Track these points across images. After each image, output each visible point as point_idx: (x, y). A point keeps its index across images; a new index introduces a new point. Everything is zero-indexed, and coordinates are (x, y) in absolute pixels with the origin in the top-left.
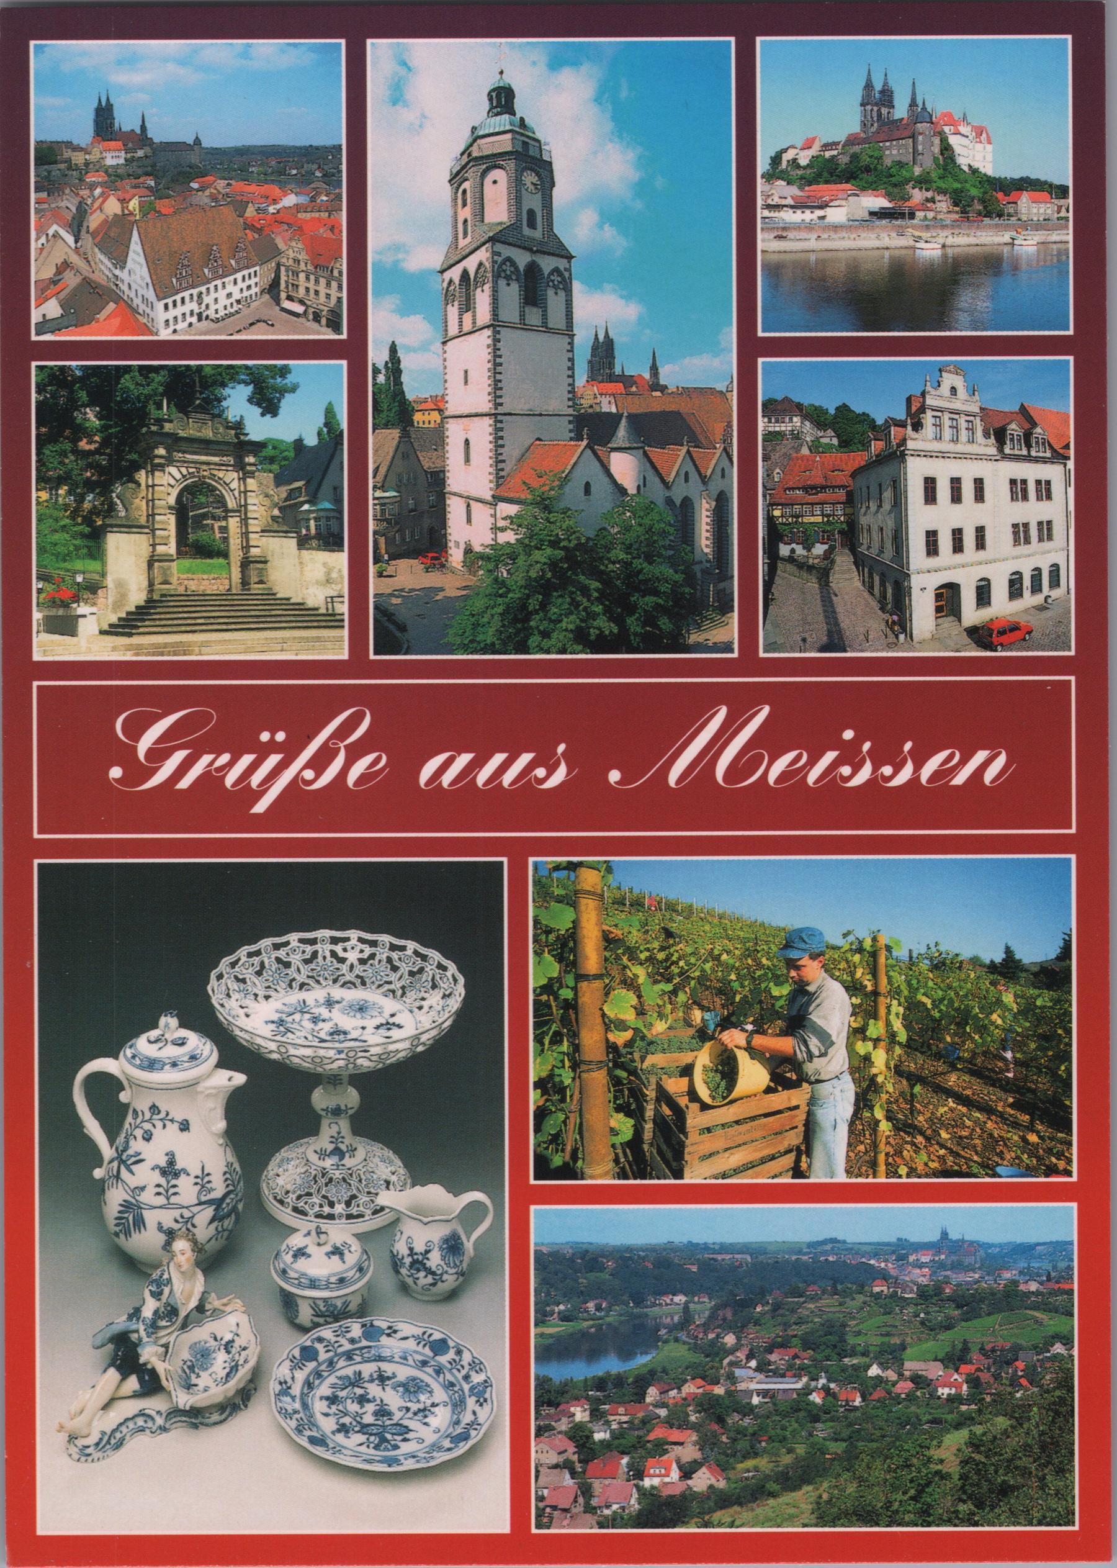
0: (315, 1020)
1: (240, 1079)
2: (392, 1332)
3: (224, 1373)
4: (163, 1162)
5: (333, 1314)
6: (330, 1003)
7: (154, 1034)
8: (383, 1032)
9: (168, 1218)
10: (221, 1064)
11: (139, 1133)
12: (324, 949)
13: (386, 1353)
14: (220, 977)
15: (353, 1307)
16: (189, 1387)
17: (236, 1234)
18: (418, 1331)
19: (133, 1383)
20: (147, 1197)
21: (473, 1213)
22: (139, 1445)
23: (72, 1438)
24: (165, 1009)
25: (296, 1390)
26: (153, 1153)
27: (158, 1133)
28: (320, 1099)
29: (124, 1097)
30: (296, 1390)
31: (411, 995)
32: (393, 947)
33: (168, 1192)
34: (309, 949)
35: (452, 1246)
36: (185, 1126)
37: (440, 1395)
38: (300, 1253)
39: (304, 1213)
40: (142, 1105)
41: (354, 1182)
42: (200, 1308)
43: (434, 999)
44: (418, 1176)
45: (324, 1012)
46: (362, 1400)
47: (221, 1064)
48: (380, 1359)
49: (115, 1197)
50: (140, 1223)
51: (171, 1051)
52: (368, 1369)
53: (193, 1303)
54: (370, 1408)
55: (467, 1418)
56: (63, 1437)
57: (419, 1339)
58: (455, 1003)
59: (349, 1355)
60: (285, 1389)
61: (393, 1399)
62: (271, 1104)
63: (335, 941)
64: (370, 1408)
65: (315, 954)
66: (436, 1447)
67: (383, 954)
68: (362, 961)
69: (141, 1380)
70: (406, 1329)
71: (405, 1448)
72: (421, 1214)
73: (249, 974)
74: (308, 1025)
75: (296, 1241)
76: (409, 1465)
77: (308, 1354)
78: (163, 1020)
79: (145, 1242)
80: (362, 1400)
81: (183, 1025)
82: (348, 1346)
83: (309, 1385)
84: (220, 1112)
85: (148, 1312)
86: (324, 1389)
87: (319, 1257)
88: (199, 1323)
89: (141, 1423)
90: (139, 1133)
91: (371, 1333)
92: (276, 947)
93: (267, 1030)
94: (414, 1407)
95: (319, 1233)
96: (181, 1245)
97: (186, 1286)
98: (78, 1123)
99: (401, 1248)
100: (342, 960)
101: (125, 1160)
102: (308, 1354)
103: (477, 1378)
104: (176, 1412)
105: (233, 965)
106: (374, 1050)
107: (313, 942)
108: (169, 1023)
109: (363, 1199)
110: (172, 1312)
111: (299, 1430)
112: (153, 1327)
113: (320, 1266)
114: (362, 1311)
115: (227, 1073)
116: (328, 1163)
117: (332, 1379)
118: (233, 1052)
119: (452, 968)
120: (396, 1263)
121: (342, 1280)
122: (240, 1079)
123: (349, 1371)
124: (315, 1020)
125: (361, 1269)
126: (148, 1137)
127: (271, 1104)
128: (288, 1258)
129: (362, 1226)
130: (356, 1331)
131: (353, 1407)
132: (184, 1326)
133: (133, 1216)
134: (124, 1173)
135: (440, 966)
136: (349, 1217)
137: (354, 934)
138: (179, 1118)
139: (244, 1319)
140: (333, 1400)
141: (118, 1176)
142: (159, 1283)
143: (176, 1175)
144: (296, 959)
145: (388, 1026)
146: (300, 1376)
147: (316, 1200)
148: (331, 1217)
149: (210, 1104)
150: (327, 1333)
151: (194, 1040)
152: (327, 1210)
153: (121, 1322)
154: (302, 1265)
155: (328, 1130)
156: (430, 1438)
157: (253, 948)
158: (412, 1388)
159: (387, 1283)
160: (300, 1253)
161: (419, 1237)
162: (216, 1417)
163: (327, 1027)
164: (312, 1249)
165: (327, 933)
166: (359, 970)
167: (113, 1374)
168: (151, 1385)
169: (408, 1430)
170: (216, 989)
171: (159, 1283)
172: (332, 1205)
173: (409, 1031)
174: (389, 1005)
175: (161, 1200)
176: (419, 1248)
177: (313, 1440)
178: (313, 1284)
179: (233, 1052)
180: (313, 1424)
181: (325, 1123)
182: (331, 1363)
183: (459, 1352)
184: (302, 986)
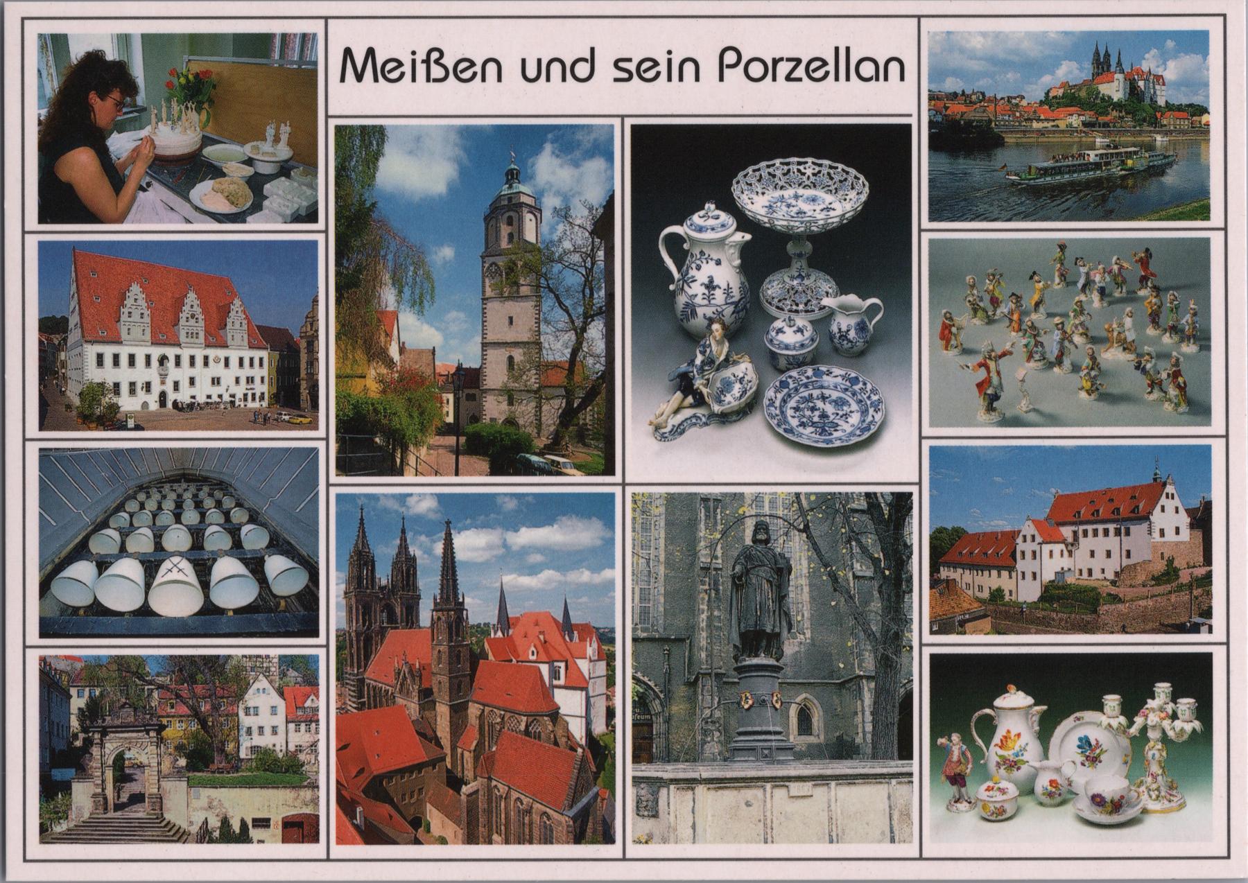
0: (789, 206)
1: (748, 237)
2: (829, 373)
3: (738, 395)
4: (706, 281)
5: (798, 363)
6: (796, 197)
7: (702, 213)
8: (825, 213)
9: (709, 311)
10: (738, 229)
11: (694, 266)
12: (794, 168)
13: (826, 384)
14: (738, 182)
15: (808, 359)
16: (720, 402)
17: (746, 323)
18: (843, 373)
19: (690, 399)
20: (698, 300)
21: (873, 310)
22: (692, 432)
23: (657, 428)
24: (709, 200)
25: (777, 404)
26: (701, 276)
27: (704, 266)
28: (791, 248)
29: (686, 246)
30: (777, 404)
31: (841, 193)
32: (831, 167)
33: (709, 298)
34: (786, 168)
35: (861, 327)
36: (718, 263)
37: (854, 406)
38: (780, 331)
39: (782, 309)
40: (696, 251)
41: (809, 292)
42: (727, 360)
43: (852, 194)
44: (843, 291)
45: (794, 203)
46: (813, 409)
47: (738, 229)
48: (822, 387)
49: (682, 300)
50: (694, 313)
51: (711, 222)
52: (816, 393)
53: (722, 358)
54: (817, 413)
55: (870, 419)
56: (651, 428)
57: (843, 377)
58: (864, 198)
59: (806, 386)
60: (772, 403)
61: (830, 409)
62: (765, 251)
63: (799, 163)
64: (817, 413)
65: (789, 171)
66: (852, 434)
67: (825, 171)
68: (814, 175)
69: (694, 398)
70: (837, 371)
71: (836, 434)
72: (845, 309)
73: (753, 181)
74: (785, 209)
75: (778, 324)
76: (838, 444)
77: (784, 384)
78: (707, 206)
79: (699, 322)
80: (813, 409)
81: (717, 208)
82: (805, 381)
83: (784, 401)
84: (737, 255)
85: (698, 361)
86: (792, 403)
87: (790, 335)
88: (726, 367)
89: (693, 422)
90: (694, 266)
91: (817, 373)
92: (768, 166)
93: (763, 211)
94: (841, 413)
95: (790, 320)
96: (716, 326)
97: (720, 350)
98: (663, 261)
99: (834, 328)
100: (804, 174)
101: (686, 280)
102: (784, 384)
103: (875, 398)
104: (712, 415)
105: (745, 176)
106: (821, 222)
107: (788, 164)
108: (710, 206)
109: (814, 302)
110: (710, 361)
111: (779, 425)
112: (701, 370)
113: (790, 337)
114: (813, 362)
115: (741, 234)
116: (795, 282)
117: (797, 398)
118: (744, 222)
119: (862, 178)
120: (831, 337)
121: (802, 346)
122: (748, 237)
123: (806, 394)
124: (789, 206)
125: (812, 340)
126: (699, 268)
127: (765, 251)
128: (774, 334)
129: (812, 316)
130: (810, 372)
131: (808, 413)
132: (718, 370)
133: (691, 309)
134: (686, 287)
135: (856, 177)
136: (807, 311)
137: (810, 160)
138: (715, 257)
139: (750, 366)
140: (797, 409)
141: (682, 289)
142: (704, 346)
143: (714, 288)
144: (778, 173)
145: (828, 209)
146: (780, 396)
147: (788, 302)
148: (797, 311)
149: (732, 251)
150: (794, 373)
151: (724, 217)
152: (794, 307)
153: (684, 367)
154: (781, 337)
155: (796, 265)
156: (849, 429)
157: (756, 167)
158: (839, 403)
159: (827, 348)
160: (780, 331)
161: (844, 323)
162: (734, 418)
163: (795, 210)
164: (786, 329)
165: (796, 159)
166: (812, 179)
167: (679, 395)
168: (700, 401)
169: (837, 425)
170: (736, 190)
171: (704, 346)
172: (797, 305)
173: (839, 212)
174: (829, 198)
175: (706, 302)
176: (844, 328)
177: (785, 430)
178: (787, 347)
179: (744, 222)
180: (786, 422)
181: (794, 261)
182: (796, 390)
183: (865, 384)
184: (782, 188)
